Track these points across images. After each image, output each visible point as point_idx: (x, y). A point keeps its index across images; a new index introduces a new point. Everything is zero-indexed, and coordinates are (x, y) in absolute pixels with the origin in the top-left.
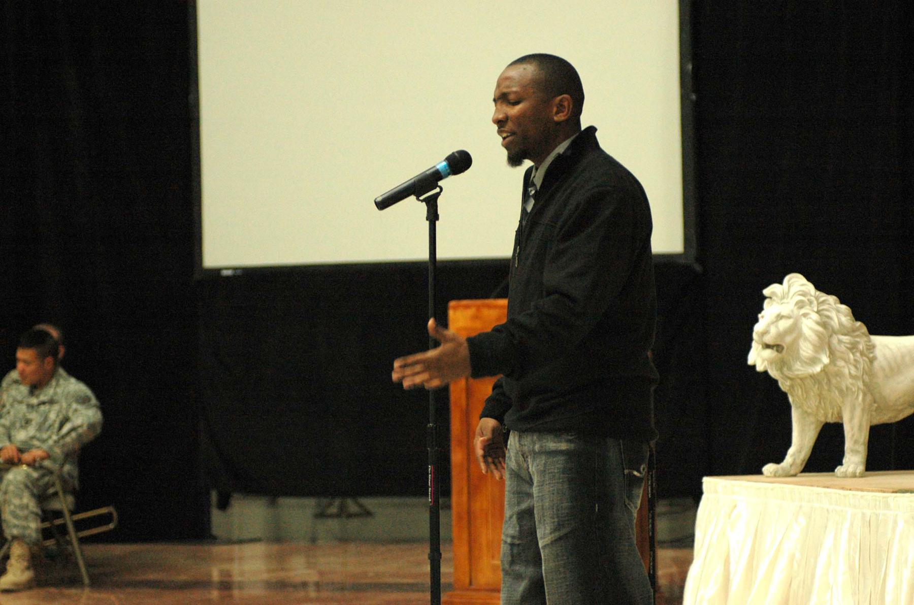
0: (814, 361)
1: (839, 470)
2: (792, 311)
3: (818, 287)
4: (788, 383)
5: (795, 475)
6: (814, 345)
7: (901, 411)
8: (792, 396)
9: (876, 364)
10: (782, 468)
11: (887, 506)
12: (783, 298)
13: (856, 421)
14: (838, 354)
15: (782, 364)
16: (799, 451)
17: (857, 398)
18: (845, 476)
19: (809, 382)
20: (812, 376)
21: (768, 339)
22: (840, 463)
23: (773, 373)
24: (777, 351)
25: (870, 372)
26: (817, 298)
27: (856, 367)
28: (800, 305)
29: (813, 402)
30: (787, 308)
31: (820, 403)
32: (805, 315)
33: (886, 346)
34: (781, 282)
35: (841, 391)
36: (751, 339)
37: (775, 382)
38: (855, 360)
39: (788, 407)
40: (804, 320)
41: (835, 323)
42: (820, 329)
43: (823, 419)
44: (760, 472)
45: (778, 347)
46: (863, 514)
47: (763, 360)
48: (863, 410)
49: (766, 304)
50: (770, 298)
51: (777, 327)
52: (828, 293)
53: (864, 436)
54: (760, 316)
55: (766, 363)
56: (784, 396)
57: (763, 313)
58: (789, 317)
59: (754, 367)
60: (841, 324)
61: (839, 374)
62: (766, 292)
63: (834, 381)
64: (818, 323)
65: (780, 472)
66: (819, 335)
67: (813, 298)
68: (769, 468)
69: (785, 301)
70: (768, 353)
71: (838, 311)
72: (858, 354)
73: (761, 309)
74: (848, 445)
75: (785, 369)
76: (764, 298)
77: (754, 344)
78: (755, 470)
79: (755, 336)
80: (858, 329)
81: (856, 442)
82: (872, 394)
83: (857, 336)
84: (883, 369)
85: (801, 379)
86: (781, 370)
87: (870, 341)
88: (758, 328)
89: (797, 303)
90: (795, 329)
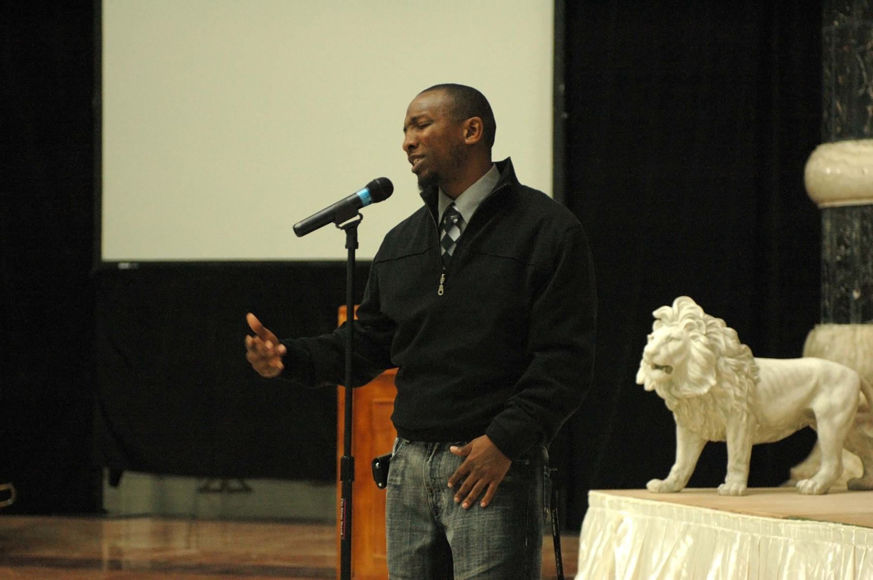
0: (701, 382)
1: (722, 488)
2: (682, 333)
3: (707, 311)
4: (676, 403)
5: (678, 492)
6: (702, 367)
7: (783, 431)
8: (678, 415)
9: (760, 386)
11: (778, 532)
12: (673, 320)
13: (739, 441)
14: (724, 376)
15: (670, 384)
16: (683, 468)
17: (741, 419)
18: (728, 494)
19: (695, 402)
20: (700, 398)
21: (658, 360)
22: (722, 481)
23: (661, 393)
24: (667, 372)
25: (754, 394)
26: (705, 321)
27: (741, 389)
28: (689, 327)
29: (699, 421)
30: (676, 330)
31: (705, 422)
32: (694, 338)
33: (770, 369)
34: (670, 305)
35: (725, 411)
36: (639, 357)
37: (662, 401)
38: (741, 383)
39: (672, 426)
40: (693, 342)
41: (722, 346)
42: (708, 351)
43: (707, 438)
45: (667, 368)
46: (753, 538)
47: (652, 380)
48: (747, 430)
49: (655, 325)
50: (660, 319)
51: (666, 348)
52: (716, 316)
53: (747, 455)
55: (654, 383)
56: (670, 414)
57: (653, 334)
58: (678, 339)
60: (727, 347)
61: (724, 396)
62: (656, 313)
63: (719, 402)
64: (706, 346)
65: (665, 488)
66: (707, 358)
67: (702, 322)
68: (653, 484)
69: (675, 323)
70: (657, 374)
71: (725, 334)
72: (743, 377)
73: (650, 331)
74: (731, 464)
75: (673, 389)
77: (642, 363)
78: (640, 484)
79: (645, 355)
80: (744, 351)
81: (739, 461)
82: (755, 415)
83: (743, 359)
85: (688, 399)
86: (668, 390)
87: (754, 363)
88: (649, 349)
89: (686, 326)
90: (684, 351)
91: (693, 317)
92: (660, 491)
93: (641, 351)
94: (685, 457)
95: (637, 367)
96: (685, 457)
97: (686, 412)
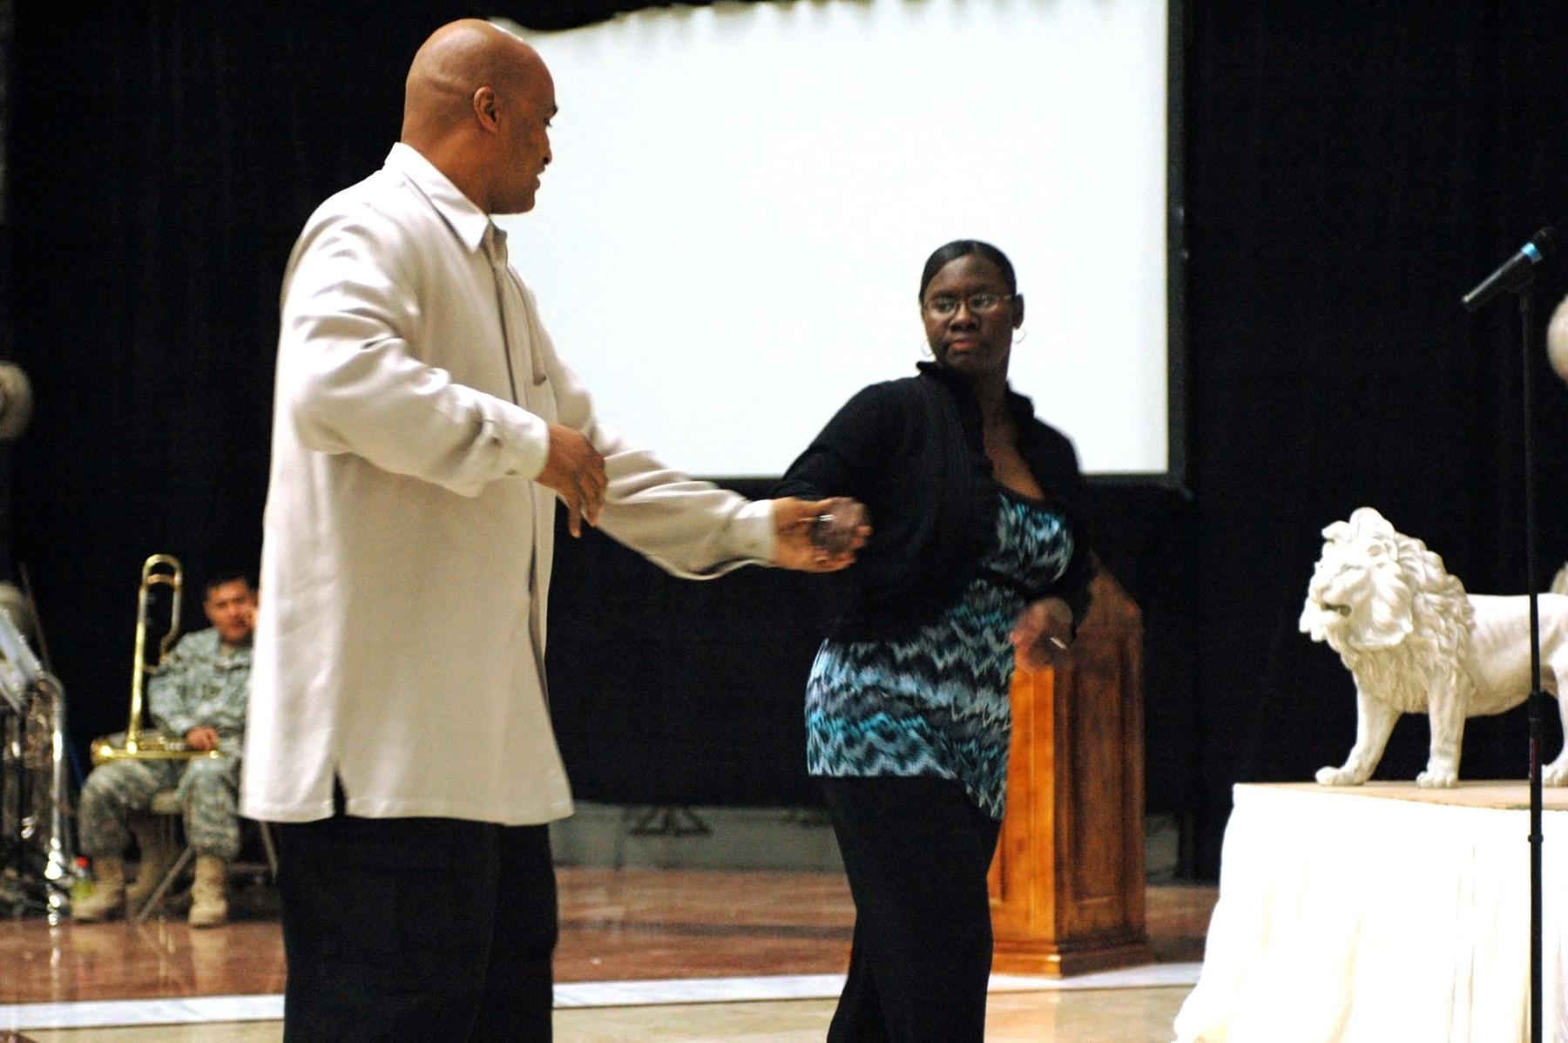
0: (1390, 628)
1: (1422, 778)
4: (1355, 658)
5: (1360, 784)
6: (1392, 607)
7: (1509, 698)
8: (1360, 675)
9: (1475, 634)
10: (1344, 775)
12: (1350, 541)
13: (1447, 712)
14: (1424, 620)
15: (1347, 632)
16: (1368, 750)
18: (1431, 786)
19: (1383, 657)
20: (1389, 651)
21: (1330, 597)
22: (1424, 769)
23: (1335, 644)
25: (1467, 645)
26: (1397, 542)
27: (1448, 638)
29: (1389, 684)
32: (1380, 565)
34: (1346, 519)
35: (1427, 670)
36: (1304, 594)
37: (1337, 656)
38: (1448, 629)
41: (1421, 578)
42: (1401, 585)
43: (1400, 708)
44: (1312, 779)
45: (1343, 609)
48: (1457, 696)
49: (1326, 549)
52: (1411, 534)
53: (1457, 732)
54: (1317, 565)
59: (1308, 635)
60: (1429, 579)
61: (1425, 647)
62: (1327, 532)
63: (1417, 656)
64: (1399, 577)
65: (1341, 779)
66: (1400, 594)
68: (1325, 774)
70: (1332, 617)
72: (1451, 620)
73: (1318, 557)
74: (1435, 744)
75: (1352, 639)
76: (1323, 541)
79: (1312, 590)
81: (1446, 740)
83: (1452, 596)
84: (1485, 642)
85: (1374, 653)
86: (1345, 639)
87: (1466, 602)
88: (1315, 583)
90: (1365, 584)
91: (1380, 537)
92: (1335, 783)
93: (1307, 585)
94: (1371, 735)
95: (1300, 608)
96: (1371, 735)
97: (1371, 670)
